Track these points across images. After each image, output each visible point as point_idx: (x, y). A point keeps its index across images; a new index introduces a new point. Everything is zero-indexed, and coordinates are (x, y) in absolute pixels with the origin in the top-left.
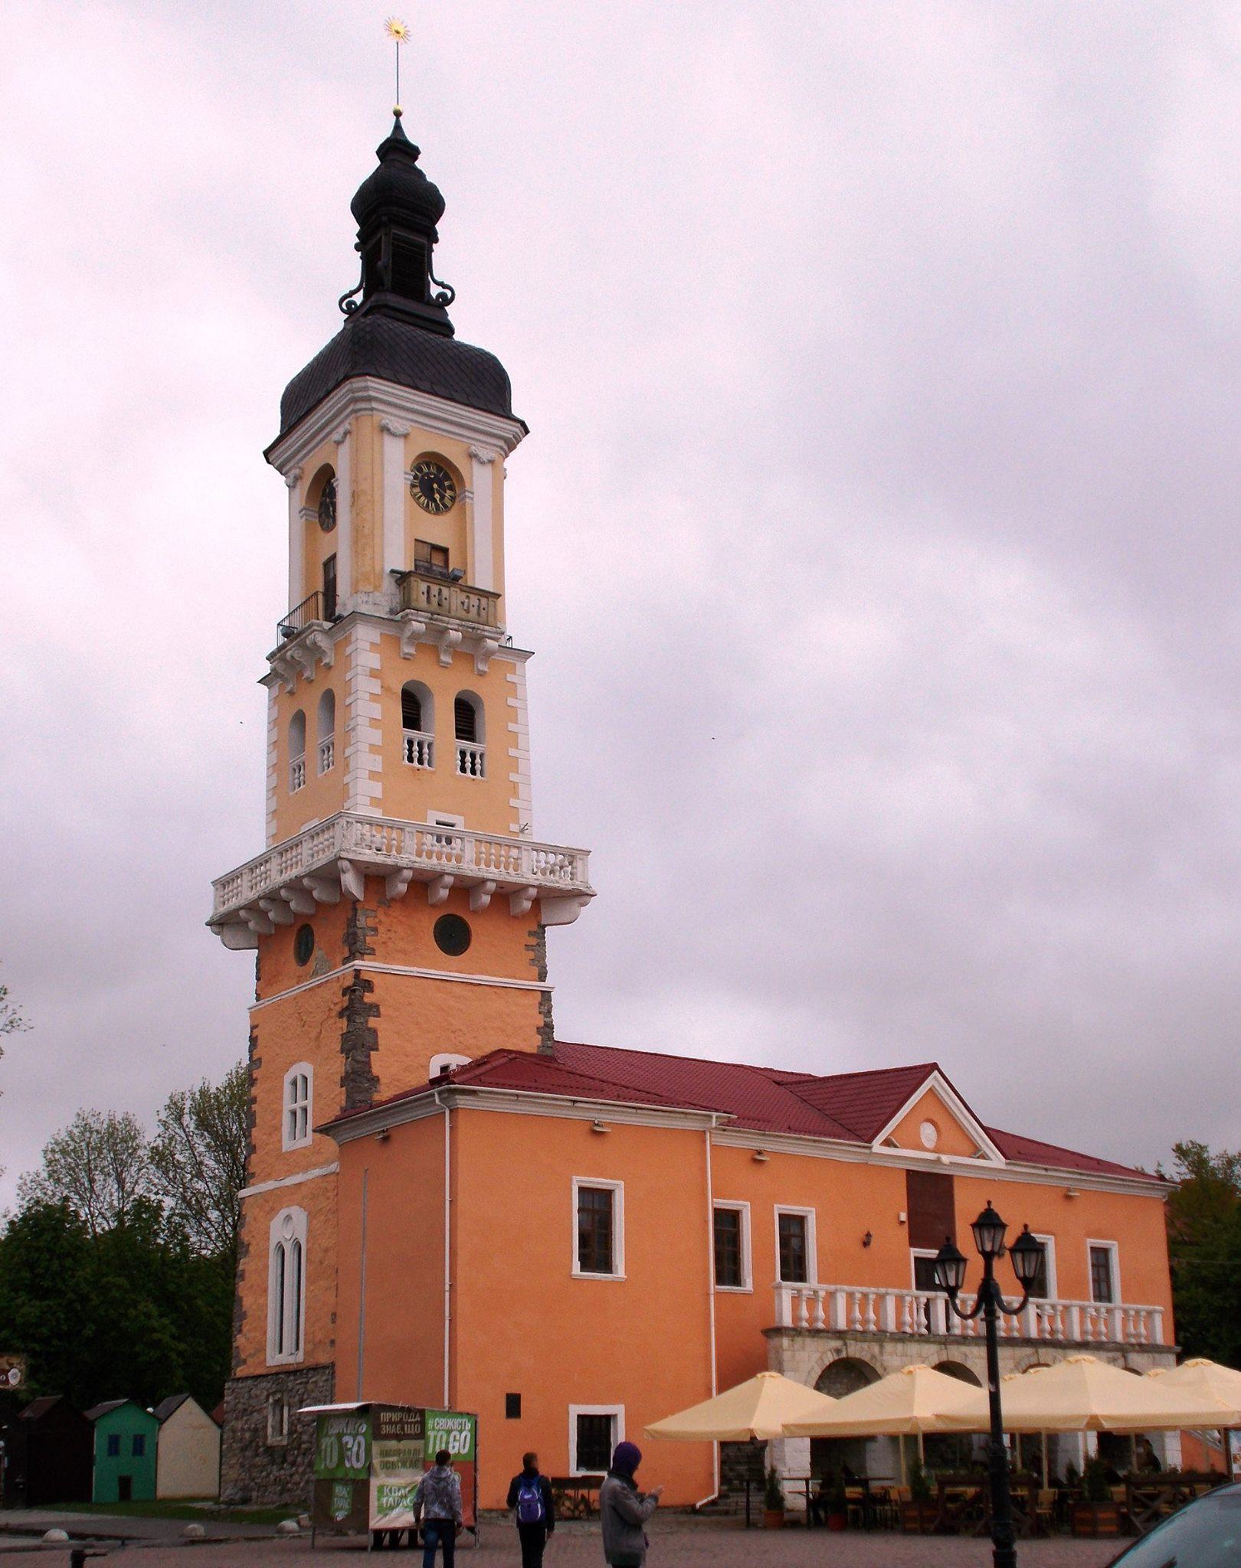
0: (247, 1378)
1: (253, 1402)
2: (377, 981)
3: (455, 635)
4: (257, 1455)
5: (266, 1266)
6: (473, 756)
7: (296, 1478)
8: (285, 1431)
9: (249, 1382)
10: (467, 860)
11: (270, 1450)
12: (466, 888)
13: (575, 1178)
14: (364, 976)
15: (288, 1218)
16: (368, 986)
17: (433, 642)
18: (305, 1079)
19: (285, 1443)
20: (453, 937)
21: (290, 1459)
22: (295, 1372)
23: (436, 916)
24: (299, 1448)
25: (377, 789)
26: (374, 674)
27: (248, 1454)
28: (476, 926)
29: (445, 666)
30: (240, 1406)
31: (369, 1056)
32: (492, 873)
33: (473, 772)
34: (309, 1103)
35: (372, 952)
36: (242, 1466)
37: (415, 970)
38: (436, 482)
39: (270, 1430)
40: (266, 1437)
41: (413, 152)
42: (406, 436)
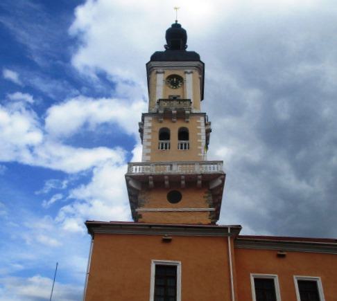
2: (144, 215)
3: (174, 112)
6: (185, 144)
10: (177, 170)
12: (175, 180)
13: (152, 261)
14: (139, 213)
16: (140, 216)
17: (167, 115)
20: (174, 198)
23: (168, 192)
25: (148, 158)
26: (149, 128)
28: (183, 194)
29: (174, 122)
32: (184, 172)
33: (185, 148)
35: (143, 206)
37: (158, 210)
38: (175, 81)
41: (179, 26)
42: (163, 72)
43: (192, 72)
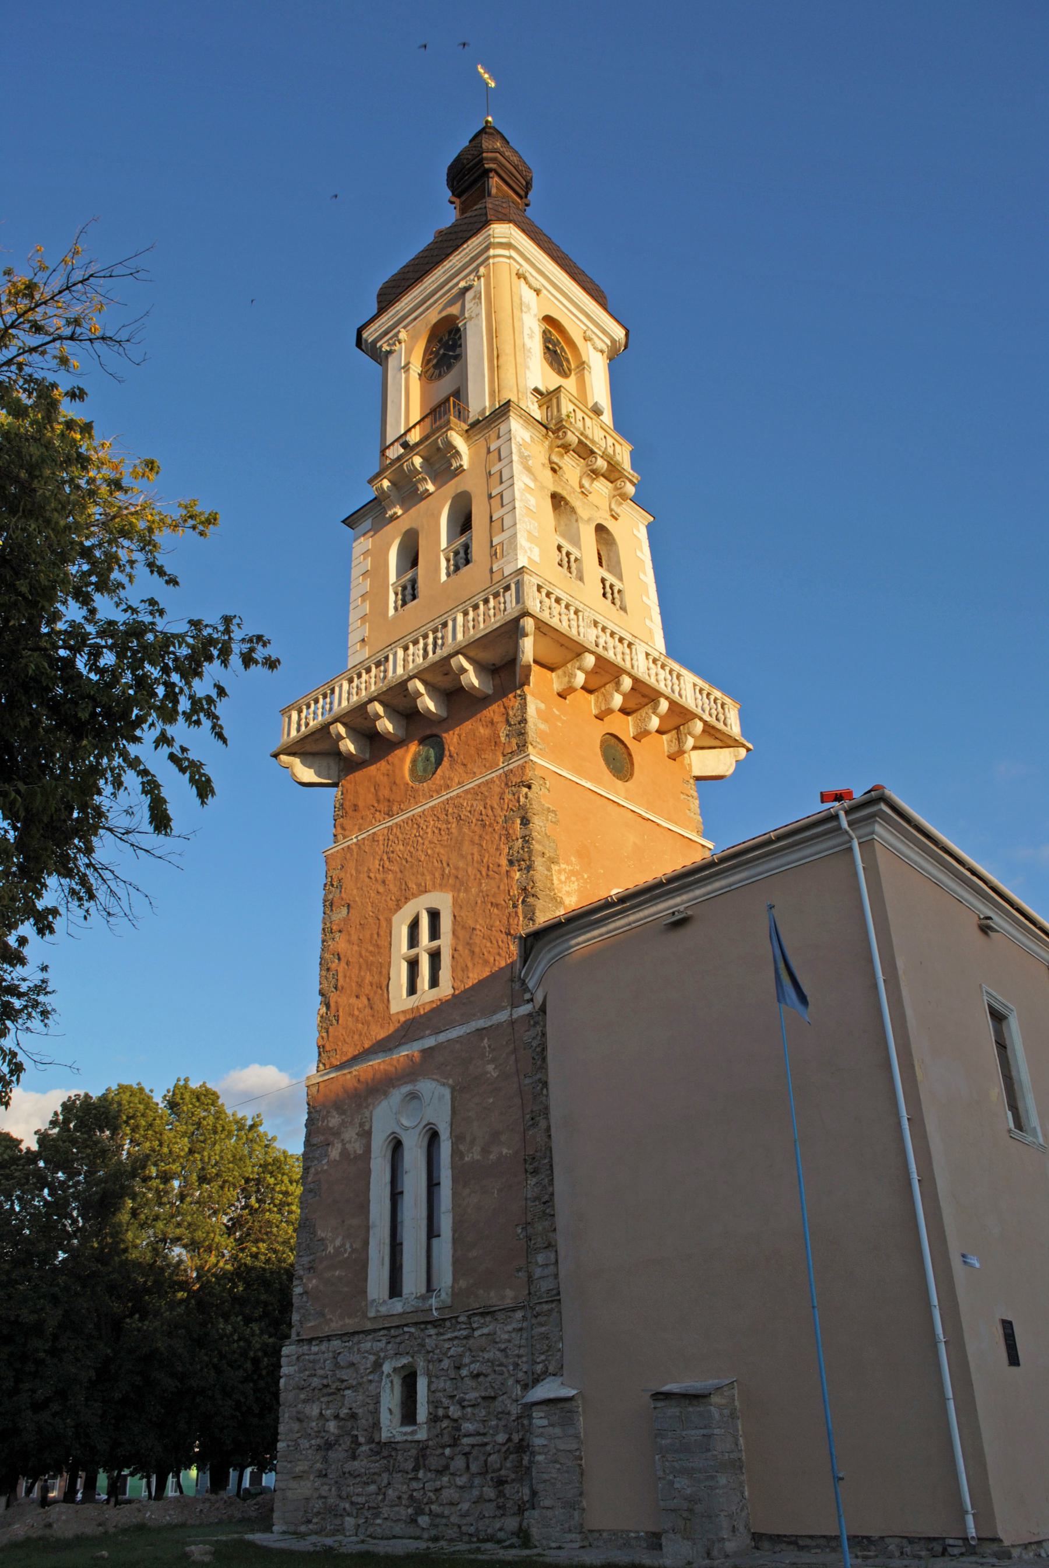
0: (329, 1338)
1: (343, 1374)
4: (354, 1458)
5: (368, 1172)
7: (447, 1494)
8: (422, 1413)
9: (336, 1343)
11: (385, 1449)
15: (413, 1096)
18: (434, 916)
19: (422, 1435)
21: (434, 1462)
22: (435, 1323)
24: (455, 1443)
27: (338, 1454)
30: (316, 1382)
31: (549, 869)
34: (445, 942)
36: (322, 1475)
37: (588, 785)
39: (385, 1417)
40: (376, 1425)
43: (602, 352)
